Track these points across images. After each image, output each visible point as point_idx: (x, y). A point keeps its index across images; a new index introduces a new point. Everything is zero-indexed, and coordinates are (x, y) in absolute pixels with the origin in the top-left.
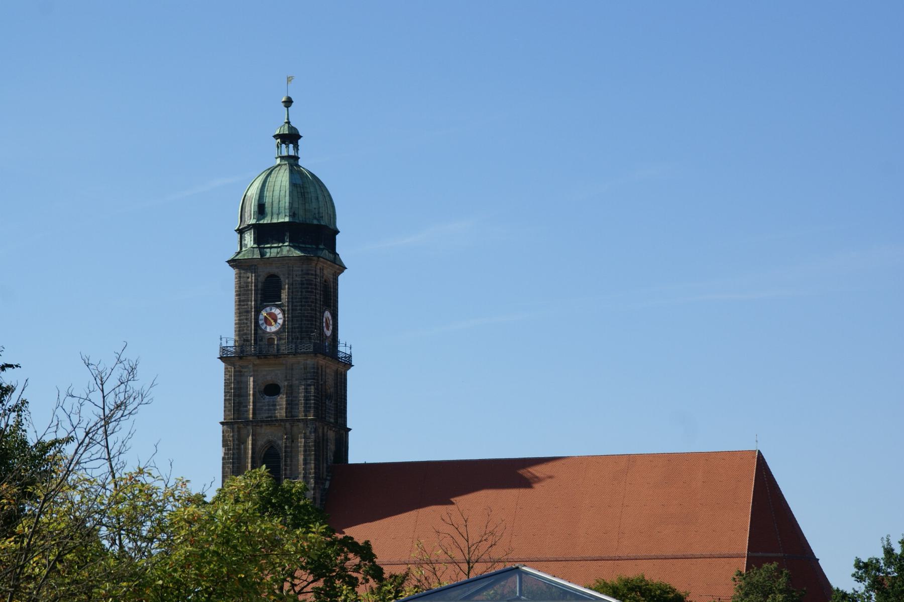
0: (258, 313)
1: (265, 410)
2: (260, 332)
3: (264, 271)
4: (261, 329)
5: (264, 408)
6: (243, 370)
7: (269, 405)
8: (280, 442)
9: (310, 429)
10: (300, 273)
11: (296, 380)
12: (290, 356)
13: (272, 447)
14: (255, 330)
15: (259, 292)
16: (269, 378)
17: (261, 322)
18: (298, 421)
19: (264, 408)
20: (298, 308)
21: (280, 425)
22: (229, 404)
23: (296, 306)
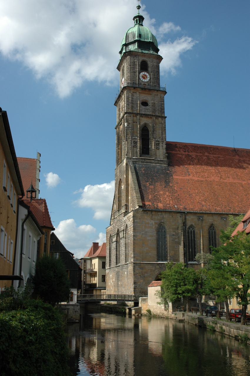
0: (139, 73)
1: (143, 111)
2: (140, 81)
3: (141, 59)
4: (141, 80)
5: (143, 110)
6: (134, 94)
7: (145, 109)
8: (150, 125)
9: (163, 121)
10: (156, 62)
11: (156, 101)
12: (156, 91)
13: (145, 126)
14: (139, 79)
15: (140, 66)
16: (145, 98)
17: (140, 77)
18: (159, 117)
19: (143, 110)
20: (156, 75)
21: (151, 117)
22: (129, 106)
23: (155, 74)
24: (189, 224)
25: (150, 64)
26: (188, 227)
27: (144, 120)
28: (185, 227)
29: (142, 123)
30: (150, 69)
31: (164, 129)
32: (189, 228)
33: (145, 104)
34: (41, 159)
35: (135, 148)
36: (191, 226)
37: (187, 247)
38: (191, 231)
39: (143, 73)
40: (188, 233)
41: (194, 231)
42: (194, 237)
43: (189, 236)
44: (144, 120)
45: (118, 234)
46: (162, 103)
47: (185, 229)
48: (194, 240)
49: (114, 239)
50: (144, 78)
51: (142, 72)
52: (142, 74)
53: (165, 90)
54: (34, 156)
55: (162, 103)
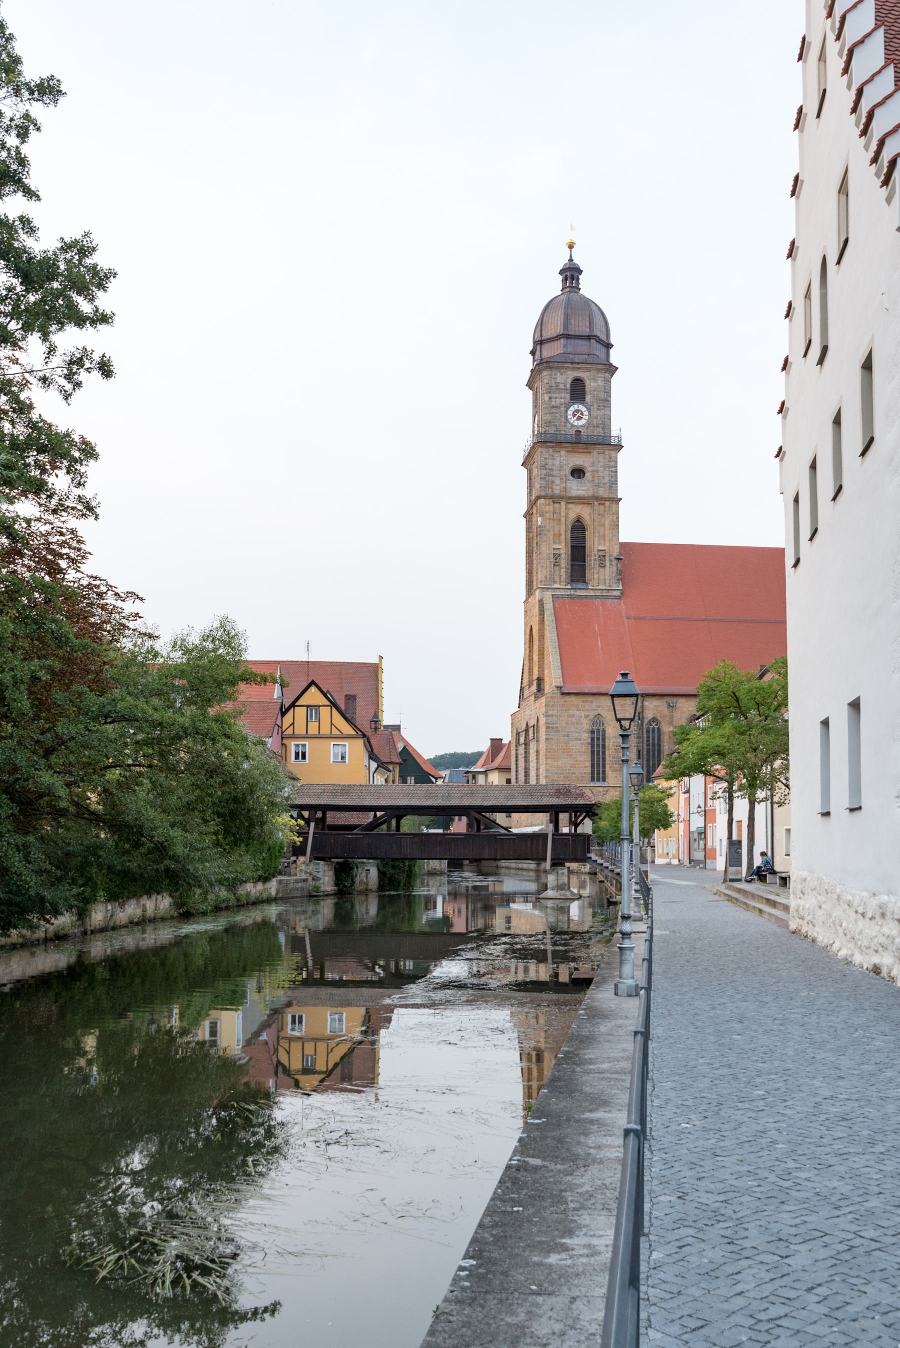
16: (577, 463)
24: (649, 715)
25: (590, 385)
26: (646, 721)
27: (575, 511)
28: (642, 722)
29: (572, 516)
30: (588, 398)
31: (616, 526)
32: (650, 723)
33: (578, 473)
34: (384, 665)
35: (556, 568)
36: (654, 720)
37: (645, 757)
38: (653, 729)
39: (576, 407)
40: (648, 732)
41: (659, 729)
42: (659, 739)
43: (648, 737)
44: (575, 511)
45: (527, 730)
46: (613, 469)
47: (642, 725)
48: (659, 745)
49: (522, 740)
50: (579, 418)
51: (574, 404)
52: (572, 409)
53: (620, 441)
54: (376, 661)
55: (613, 469)
